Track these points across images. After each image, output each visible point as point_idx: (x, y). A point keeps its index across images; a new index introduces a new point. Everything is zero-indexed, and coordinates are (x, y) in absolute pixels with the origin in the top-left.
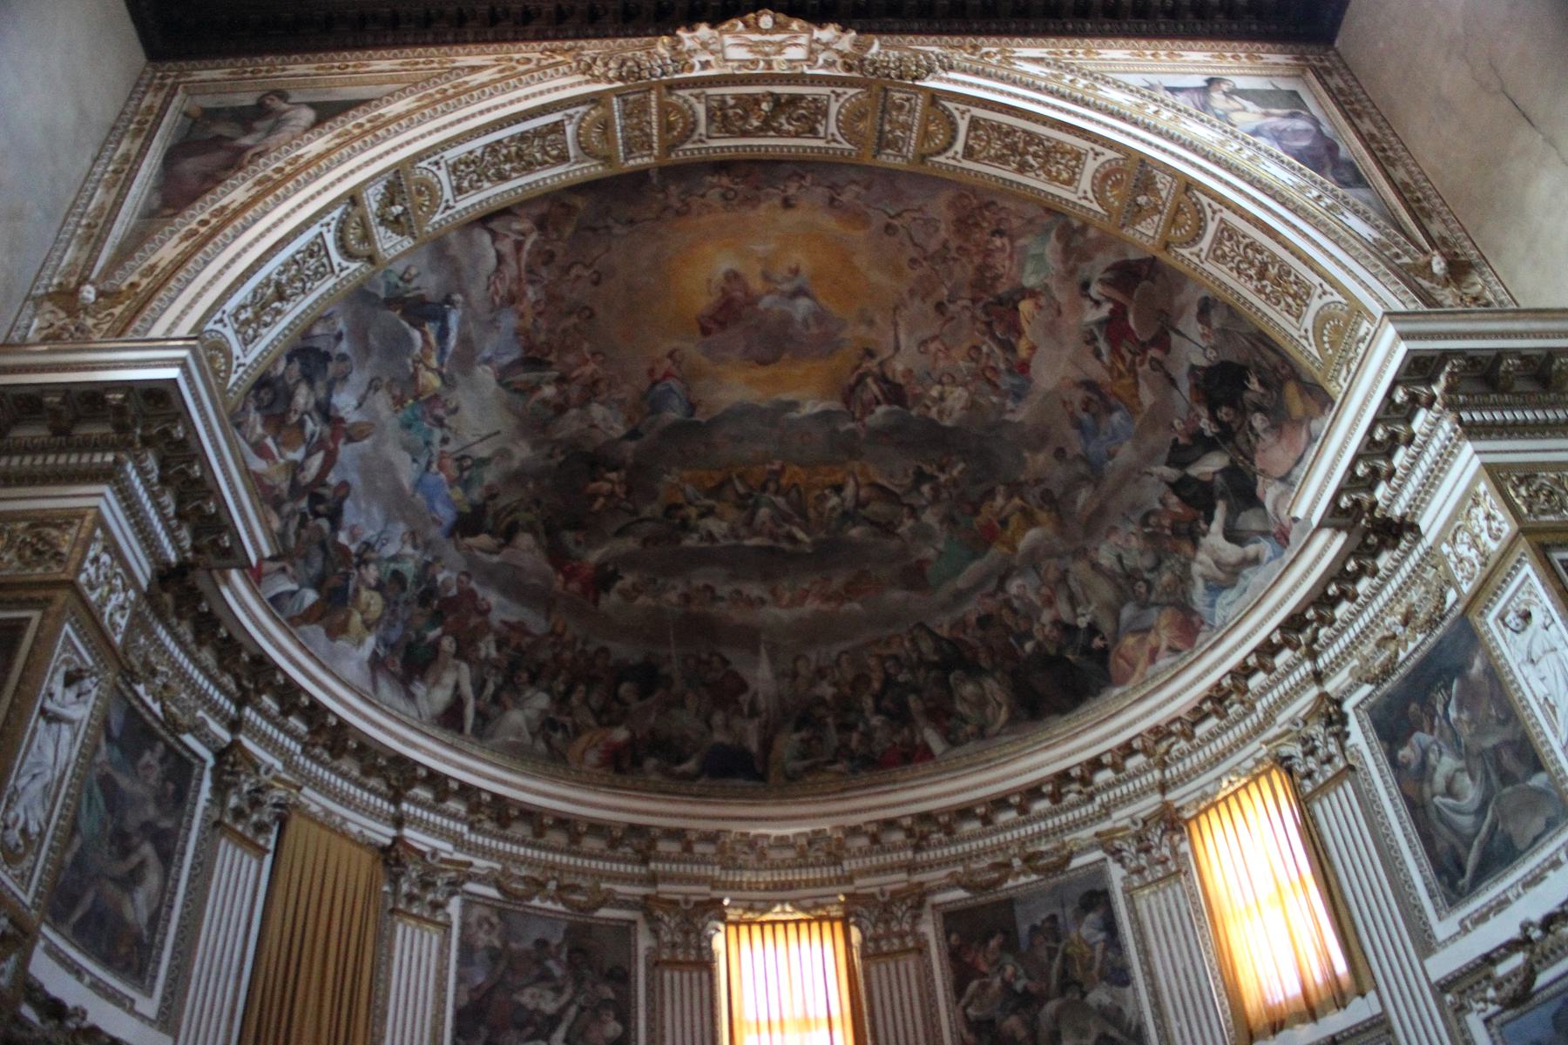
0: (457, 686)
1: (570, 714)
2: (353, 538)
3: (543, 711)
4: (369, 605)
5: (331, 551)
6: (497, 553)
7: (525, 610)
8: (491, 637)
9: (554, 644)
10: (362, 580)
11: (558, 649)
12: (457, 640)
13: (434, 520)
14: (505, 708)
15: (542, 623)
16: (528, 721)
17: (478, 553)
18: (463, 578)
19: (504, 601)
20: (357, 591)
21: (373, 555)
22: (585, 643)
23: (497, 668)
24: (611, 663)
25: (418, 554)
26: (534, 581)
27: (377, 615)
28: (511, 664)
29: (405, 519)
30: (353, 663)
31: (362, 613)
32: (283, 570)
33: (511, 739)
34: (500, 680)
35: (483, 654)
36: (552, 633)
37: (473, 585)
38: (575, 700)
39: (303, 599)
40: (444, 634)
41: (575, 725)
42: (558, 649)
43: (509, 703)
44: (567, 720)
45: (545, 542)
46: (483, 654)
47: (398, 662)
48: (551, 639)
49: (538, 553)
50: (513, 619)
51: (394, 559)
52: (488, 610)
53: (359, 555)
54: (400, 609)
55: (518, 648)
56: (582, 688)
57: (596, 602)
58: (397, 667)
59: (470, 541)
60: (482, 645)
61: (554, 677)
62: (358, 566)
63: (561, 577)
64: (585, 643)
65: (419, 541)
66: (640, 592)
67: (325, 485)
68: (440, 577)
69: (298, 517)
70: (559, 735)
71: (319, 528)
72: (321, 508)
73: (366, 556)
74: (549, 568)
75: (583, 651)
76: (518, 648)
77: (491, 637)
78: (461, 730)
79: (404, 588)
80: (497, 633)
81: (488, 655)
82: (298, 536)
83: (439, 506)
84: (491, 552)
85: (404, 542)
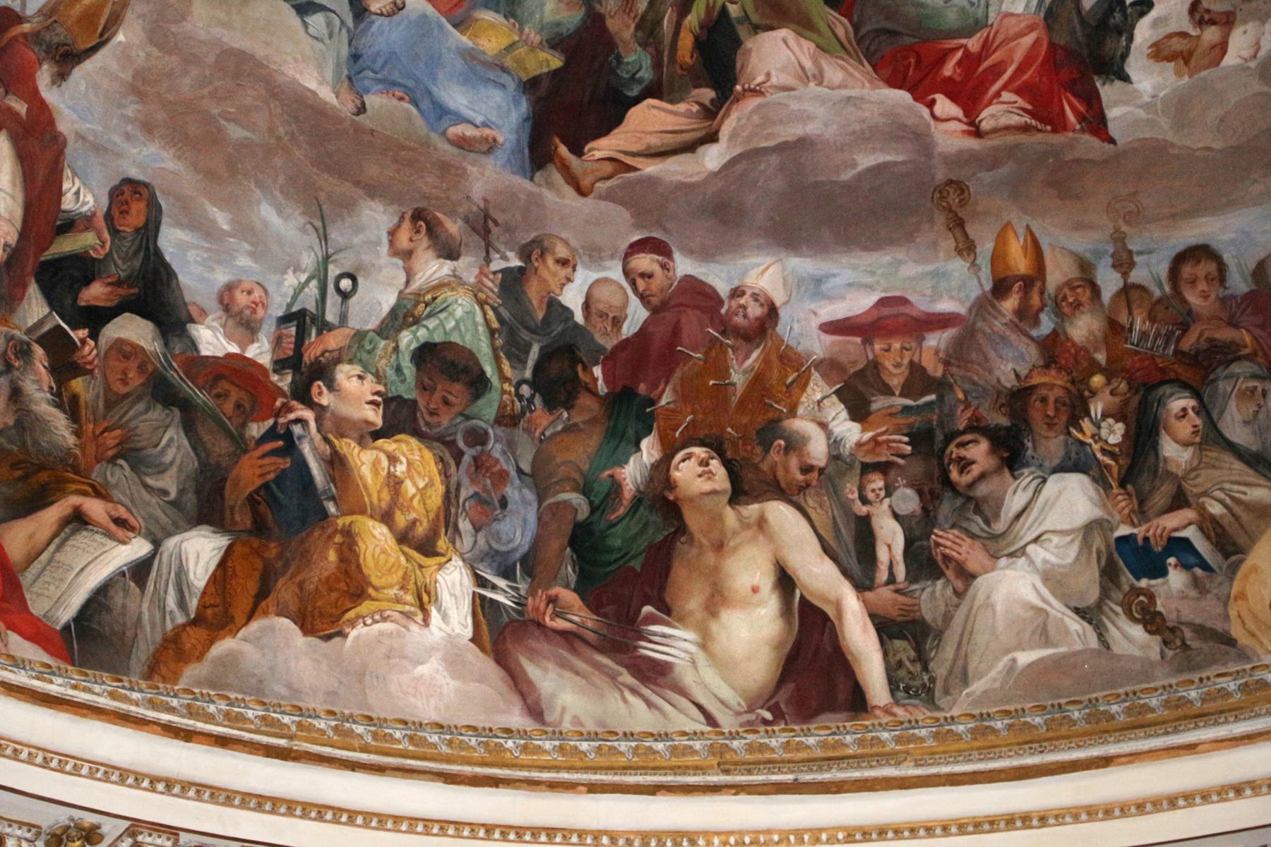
0: (785, 581)
1: (1179, 501)
2: (246, 326)
3: (1089, 529)
4: (395, 484)
5: (201, 397)
6: (712, 138)
7: (884, 258)
8: (817, 389)
9: (1026, 315)
10: (343, 427)
11: (1047, 324)
12: (717, 446)
13: (462, 144)
14: (969, 577)
15: (958, 266)
16: (1051, 578)
17: (651, 168)
18: (645, 262)
19: (802, 265)
20: (336, 463)
21: (334, 341)
22: (1124, 263)
23: (883, 468)
24: (1239, 283)
25: (467, 266)
26: (866, 161)
27: (436, 498)
28: (921, 439)
29: (373, 190)
30: (433, 669)
31: (386, 518)
32: (78, 520)
33: (1025, 658)
34: (908, 501)
35: (818, 450)
36: (1001, 288)
37: (684, 266)
38: (1174, 453)
39: (181, 572)
40: (669, 451)
41: (1210, 527)
42: (1047, 324)
43: (970, 553)
44: (1181, 523)
45: (842, 27)
46: (818, 450)
47: (569, 597)
48: (1009, 305)
49: (834, 73)
50: (860, 304)
51: (401, 317)
52: (772, 312)
53: (288, 362)
54: (496, 449)
55: (918, 380)
56: (1180, 402)
57: (1096, 123)
58: (578, 615)
59: (602, 147)
60: (801, 425)
61: (1077, 408)
62: (302, 394)
63: (944, 106)
64: (1124, 263)
65: (453, 227)
66: (1228, 21)
67: (69, 225)
68: (572, 298)
69: (39, 351)
70: (1176, 579)
71: (124, 350)
72: (95, 293)
73: (309, 355)
74: (902, 97)
75: (1128, 292)
76: (918, 380)
77: (817, 389)
78: (857, 703)
79: (478, 384)
80: (829, 367)
81: (835, 444)
82: (71, 407)
83: (456, 97)
84: (690, 147)
85: (407, 255)
